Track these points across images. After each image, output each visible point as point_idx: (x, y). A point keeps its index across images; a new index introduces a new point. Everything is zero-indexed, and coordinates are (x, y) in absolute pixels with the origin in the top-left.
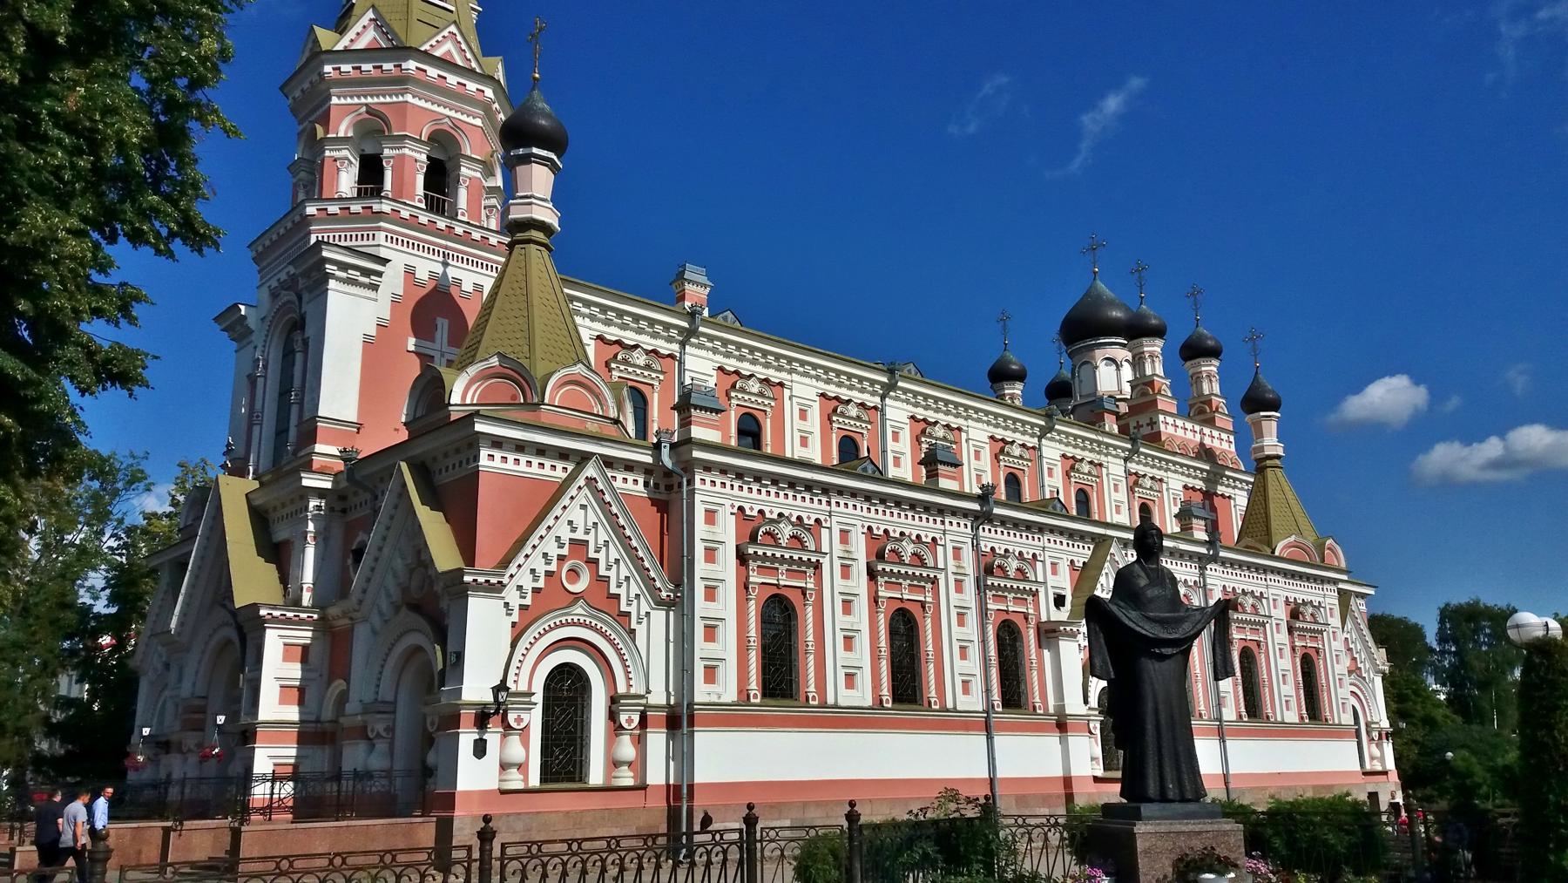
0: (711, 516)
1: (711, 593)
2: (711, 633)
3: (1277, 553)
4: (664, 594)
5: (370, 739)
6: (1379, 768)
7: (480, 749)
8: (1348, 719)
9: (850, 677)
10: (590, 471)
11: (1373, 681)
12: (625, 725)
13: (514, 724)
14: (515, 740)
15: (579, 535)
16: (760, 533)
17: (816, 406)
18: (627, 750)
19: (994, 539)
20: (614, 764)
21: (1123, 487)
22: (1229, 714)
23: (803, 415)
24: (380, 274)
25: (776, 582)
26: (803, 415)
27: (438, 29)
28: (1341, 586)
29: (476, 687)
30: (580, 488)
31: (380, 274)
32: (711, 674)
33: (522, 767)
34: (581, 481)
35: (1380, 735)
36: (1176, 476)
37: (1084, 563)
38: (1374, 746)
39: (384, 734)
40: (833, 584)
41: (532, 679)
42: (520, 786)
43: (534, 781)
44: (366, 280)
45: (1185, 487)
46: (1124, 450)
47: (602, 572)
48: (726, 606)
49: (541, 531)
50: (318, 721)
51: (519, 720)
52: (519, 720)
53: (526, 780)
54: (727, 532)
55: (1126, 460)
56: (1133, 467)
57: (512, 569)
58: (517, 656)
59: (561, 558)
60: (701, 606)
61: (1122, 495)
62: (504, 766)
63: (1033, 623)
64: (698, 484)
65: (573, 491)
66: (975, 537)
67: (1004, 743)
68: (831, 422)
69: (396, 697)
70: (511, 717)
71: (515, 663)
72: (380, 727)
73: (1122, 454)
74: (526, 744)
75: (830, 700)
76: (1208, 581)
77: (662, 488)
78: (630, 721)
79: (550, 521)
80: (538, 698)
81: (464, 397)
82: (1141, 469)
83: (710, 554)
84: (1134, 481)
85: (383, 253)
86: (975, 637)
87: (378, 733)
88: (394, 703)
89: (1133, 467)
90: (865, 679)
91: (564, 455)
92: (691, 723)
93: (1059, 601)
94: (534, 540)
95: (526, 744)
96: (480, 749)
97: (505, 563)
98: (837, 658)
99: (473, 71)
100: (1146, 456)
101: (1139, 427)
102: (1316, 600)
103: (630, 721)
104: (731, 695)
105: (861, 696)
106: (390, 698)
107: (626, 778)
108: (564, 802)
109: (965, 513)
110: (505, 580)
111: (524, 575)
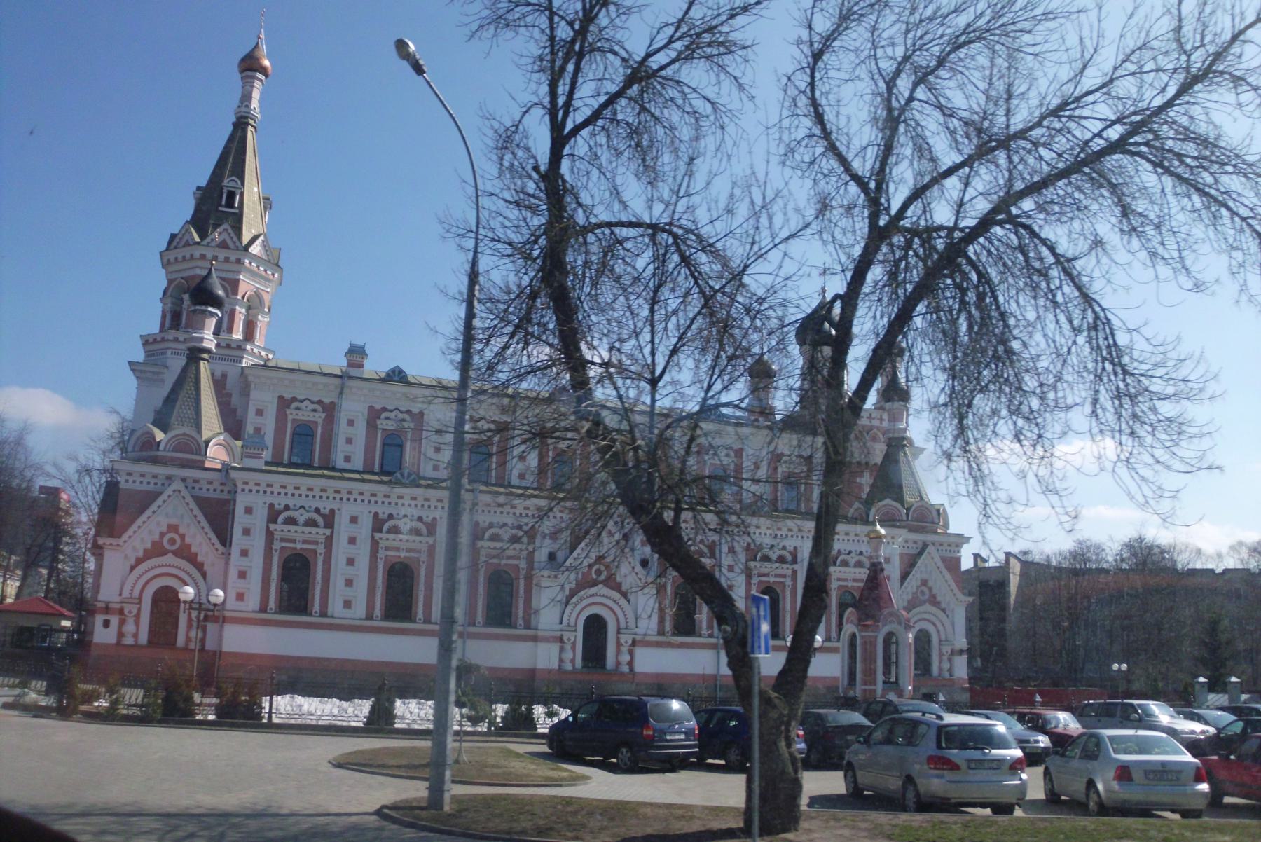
7: (106, 624)
15: (174, 521)
33: (136, 635)
34: (169, 491)
47: (188, 540)
57: (125, 537)
59: (162, 535)
62: (121, 635)
64: (239, 490)
65: (164, 497)
70: (126, 611)
74: (137, 623)
81: (134, 447)
83: (247, 532)
92: (224, 622)
93: (552, 556)
95: (137, 623)
96: (106, 624)
97: (119, 537)
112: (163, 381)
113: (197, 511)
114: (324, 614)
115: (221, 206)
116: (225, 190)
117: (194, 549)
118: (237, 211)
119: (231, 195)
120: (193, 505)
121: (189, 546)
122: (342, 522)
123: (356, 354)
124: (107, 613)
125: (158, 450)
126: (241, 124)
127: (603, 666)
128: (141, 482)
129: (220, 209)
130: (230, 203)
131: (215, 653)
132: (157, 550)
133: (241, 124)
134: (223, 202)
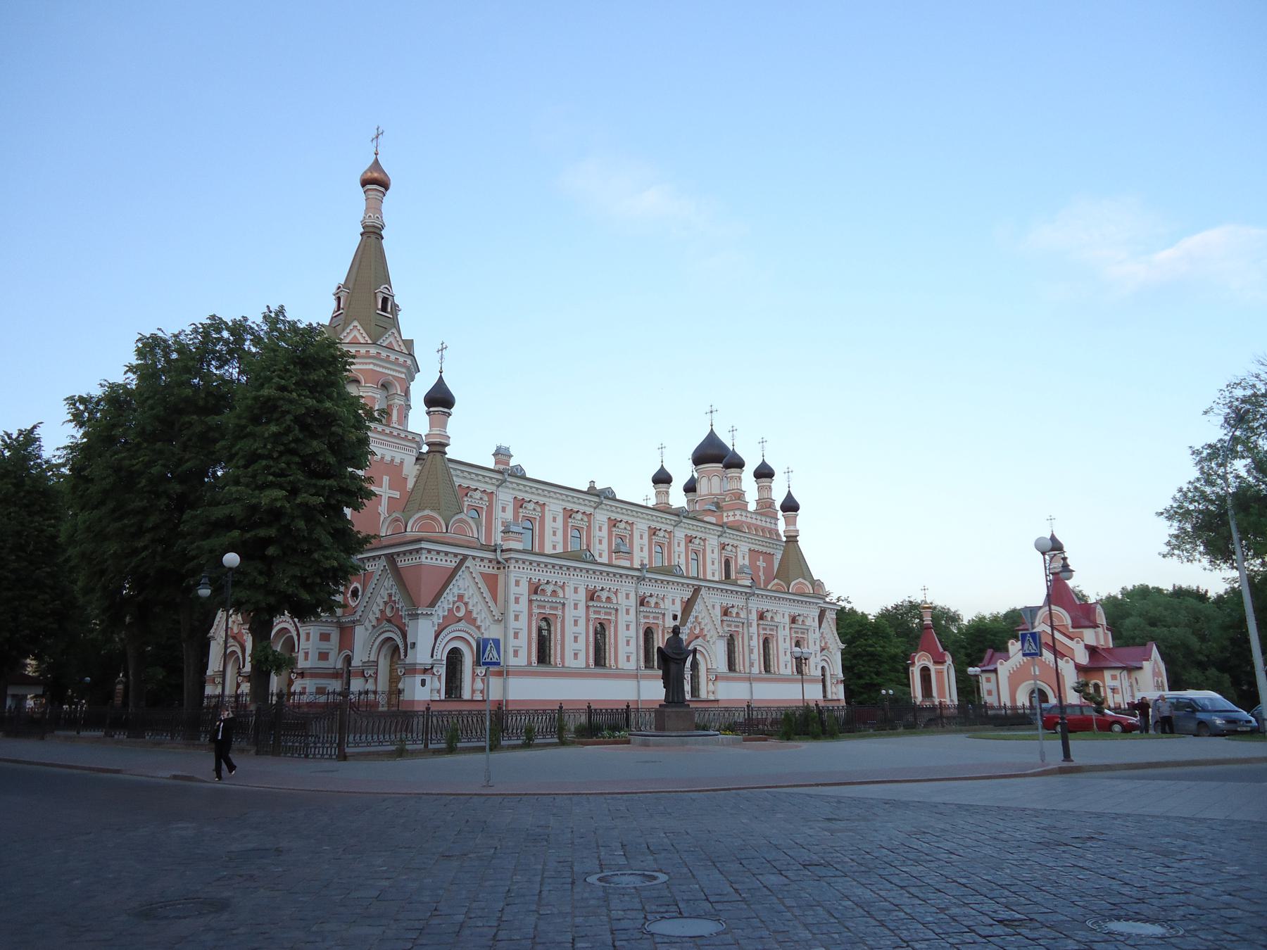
0: (517, 583)
1: (517, 618)
2: (516, 635)
3: (790, 591)
4: (496, 618)
5: (365, 677)
6: (836, 698)
7: (423, 683)
8: (819, 673)
9: (576, 655)
10: (467, 563)
11: (835, 654)
12: (479, 674)
13: (436, 673)
14: (436, 679)
15: (461, 592)
16: (540, 588)
17: (561, 515)
18: (479, 685)
19: (645, 589)
20: (473, 691)
21: (716, 551)
22: (755, 670)
23: (554, 520)
25: (544, 612)
26: (554, 520)
28: (820, 605)
29: (421, 655)
30: (463, 571)
32: (516, 653)
33: (439, 691)
34: (463, 568)
35: (837, 681)
36: (744, 543)
37: (688, 599)
38: (833, 687)
39: (373, 675)
40: (570, 613)
41: (441, 654)
42: (438, 699)
43: (443, 697)
45: (750, 550)
46: (718, 531)
47: (470, 607)
48: (523, 623)
49: (448, 591)
50: (335, 668)
51: (438, 671)
52: (438, 671)
53: (440, 696)
54: (524, 589)
55: (719, 536)
56: (723, 540)
57: (436, 607)
58: (437, 644)
59: (454, 603)
60: (513, 624)
61: (716, 555)
63: (660, 628)
66: (636, 588)
67: (643, 683)
68: (568, 522)
69: (378, 659)
71: (436, 648)
72: (371, 672)
73: (717, 534)
75: (566, 665)
76: (749, 605)
77: (495, 568)
78: (481, 673)
79: (451, 586)
80: (445, 662)
81: (412, 529)
82: (727, 541)
84: (723, 547)
86: (635, 636)
87: (370, 675)
88: (377, 662)
89: (723, 540)
90: (582, 656)
91: (456, 555)
93: (675, 617)
94: (445, 595)
96: (423, 683)
98: (570, 646)
100: (730, 534)
101: (728, 516)
102: (805, 613)
103: (481, 673)
104: (524, 662)
105: (580, 663)
106: (376, 660)
107: (478, 697)
108: (453, 706)
109: (633, 577)
110: (433, 613)
111: (442, 609)
113: (482, 584)
114: (563, 666)
117: (474, 615)
118: (391, 316)
119: (385, 300)
120: (479, 579)
121: (471, 612)
122: (569, 591)
123: (502, 454)
124: (424, 673)
125: (447, 531)
126: (372, 233)
127: (698, 696)
128: (437, 559)
129: (378, 312)
130: (384, 309)
131: (500, 703)
132: (450, 619)
133: (372, 233)
134: (380, 307)
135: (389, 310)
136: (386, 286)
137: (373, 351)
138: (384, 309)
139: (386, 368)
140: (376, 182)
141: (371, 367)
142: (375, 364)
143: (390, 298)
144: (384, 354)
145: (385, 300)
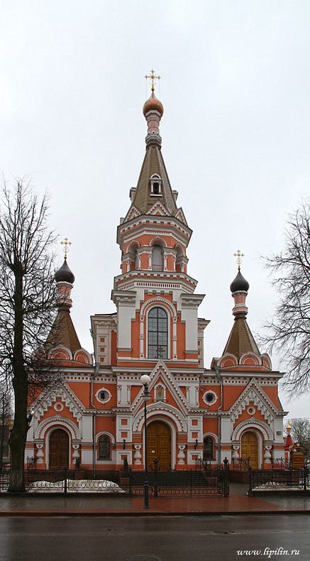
24: (135, 297)
27: (152, 205)
31: (135, 297)
44: (130, 300)
85: (135, 290)
99: (167, 216)
112: (134, 302)
115: (152, 193)
116: (152, 182)
119: (156, 186)
126: (153, 144)
130: (156, 192)
133: (153, 144)
134: (152, 191)
135: (160, 191)
136: (155, 174)
137: (144, 221)
138: (156, 192)
139: (151, 231)
140: (153, 110)
141: (145, 233)
142: (147, 231)
143: (160, 183)
144: (151, 221)
145: (156, 186)
